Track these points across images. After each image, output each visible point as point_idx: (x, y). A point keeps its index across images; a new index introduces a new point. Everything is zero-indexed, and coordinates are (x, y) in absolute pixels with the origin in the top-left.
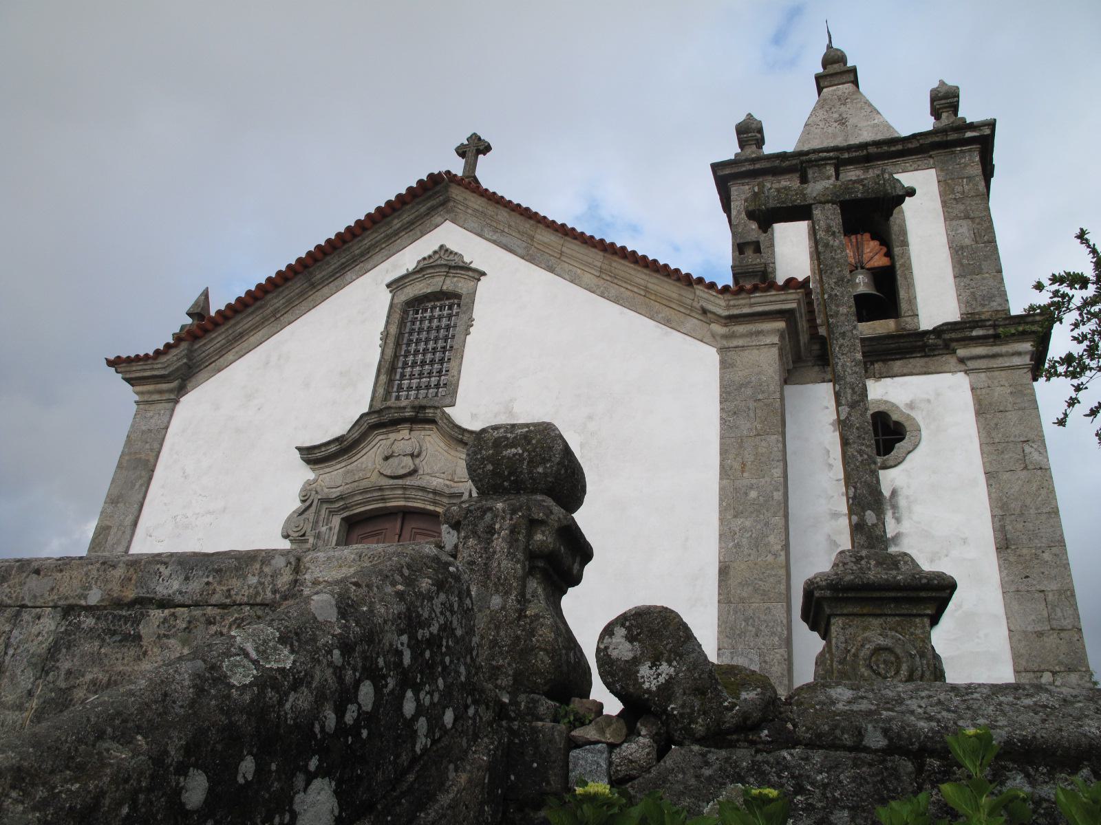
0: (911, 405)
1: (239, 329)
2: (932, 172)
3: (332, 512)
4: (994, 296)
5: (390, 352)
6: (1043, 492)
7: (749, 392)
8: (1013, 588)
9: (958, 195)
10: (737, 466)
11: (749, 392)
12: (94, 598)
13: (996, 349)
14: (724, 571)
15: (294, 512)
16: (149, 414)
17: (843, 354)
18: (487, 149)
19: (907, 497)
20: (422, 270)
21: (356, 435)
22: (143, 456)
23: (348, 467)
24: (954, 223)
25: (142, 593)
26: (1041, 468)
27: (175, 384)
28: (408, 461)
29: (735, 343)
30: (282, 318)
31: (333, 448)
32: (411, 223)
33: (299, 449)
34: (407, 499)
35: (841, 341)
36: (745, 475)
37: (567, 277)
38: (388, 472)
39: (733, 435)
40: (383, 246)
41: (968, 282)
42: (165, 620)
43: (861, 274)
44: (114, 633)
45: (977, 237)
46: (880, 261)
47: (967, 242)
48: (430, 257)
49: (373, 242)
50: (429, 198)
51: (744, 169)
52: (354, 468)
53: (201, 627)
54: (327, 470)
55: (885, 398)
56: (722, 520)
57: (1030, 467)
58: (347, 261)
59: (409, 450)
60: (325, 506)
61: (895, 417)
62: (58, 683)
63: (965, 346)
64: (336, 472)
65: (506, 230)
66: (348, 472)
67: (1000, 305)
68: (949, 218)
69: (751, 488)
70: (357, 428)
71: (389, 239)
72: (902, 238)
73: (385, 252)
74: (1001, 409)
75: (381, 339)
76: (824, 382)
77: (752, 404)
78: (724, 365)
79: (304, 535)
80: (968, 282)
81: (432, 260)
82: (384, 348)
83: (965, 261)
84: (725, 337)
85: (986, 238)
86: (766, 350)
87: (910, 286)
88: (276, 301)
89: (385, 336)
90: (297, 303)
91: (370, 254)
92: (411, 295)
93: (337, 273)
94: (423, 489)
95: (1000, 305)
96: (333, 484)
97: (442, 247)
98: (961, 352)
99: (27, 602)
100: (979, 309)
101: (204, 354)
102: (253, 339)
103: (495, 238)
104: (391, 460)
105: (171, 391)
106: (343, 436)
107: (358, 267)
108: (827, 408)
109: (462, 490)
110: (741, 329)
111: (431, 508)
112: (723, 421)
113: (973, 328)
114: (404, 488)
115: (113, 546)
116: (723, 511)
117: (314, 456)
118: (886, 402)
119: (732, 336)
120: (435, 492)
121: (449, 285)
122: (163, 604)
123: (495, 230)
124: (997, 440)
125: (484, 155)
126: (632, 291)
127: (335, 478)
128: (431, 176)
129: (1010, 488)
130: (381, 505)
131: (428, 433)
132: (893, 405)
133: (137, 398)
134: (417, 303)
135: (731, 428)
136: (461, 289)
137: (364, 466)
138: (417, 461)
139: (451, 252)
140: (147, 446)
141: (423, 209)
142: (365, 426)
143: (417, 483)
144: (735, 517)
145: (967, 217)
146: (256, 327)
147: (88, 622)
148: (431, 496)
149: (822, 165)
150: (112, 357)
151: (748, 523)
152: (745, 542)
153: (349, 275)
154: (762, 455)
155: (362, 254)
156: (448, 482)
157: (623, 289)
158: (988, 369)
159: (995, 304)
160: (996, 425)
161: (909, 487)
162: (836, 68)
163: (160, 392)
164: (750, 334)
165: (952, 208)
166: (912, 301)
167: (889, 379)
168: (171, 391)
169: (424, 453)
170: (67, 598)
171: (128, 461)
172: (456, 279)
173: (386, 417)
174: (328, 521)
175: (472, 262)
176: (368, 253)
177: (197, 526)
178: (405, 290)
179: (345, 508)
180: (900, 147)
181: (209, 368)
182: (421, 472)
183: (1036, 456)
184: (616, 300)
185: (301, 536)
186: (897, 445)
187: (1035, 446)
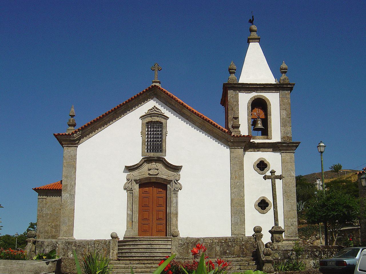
7: (237, 159)
8: (285, 202)
14: (232, 200)
48: (152, 109)
77: (237, 162)
79: (131, 189)
89: (142, 133)
98: (280, 148)
110: (235, 144)
114: (156, 178)
117: (129, 169)
118: (263, 158)
123: (170, 104)
134: (148, 123)
139: (158, 109)
159: (289, 135)
175: (164, 113)
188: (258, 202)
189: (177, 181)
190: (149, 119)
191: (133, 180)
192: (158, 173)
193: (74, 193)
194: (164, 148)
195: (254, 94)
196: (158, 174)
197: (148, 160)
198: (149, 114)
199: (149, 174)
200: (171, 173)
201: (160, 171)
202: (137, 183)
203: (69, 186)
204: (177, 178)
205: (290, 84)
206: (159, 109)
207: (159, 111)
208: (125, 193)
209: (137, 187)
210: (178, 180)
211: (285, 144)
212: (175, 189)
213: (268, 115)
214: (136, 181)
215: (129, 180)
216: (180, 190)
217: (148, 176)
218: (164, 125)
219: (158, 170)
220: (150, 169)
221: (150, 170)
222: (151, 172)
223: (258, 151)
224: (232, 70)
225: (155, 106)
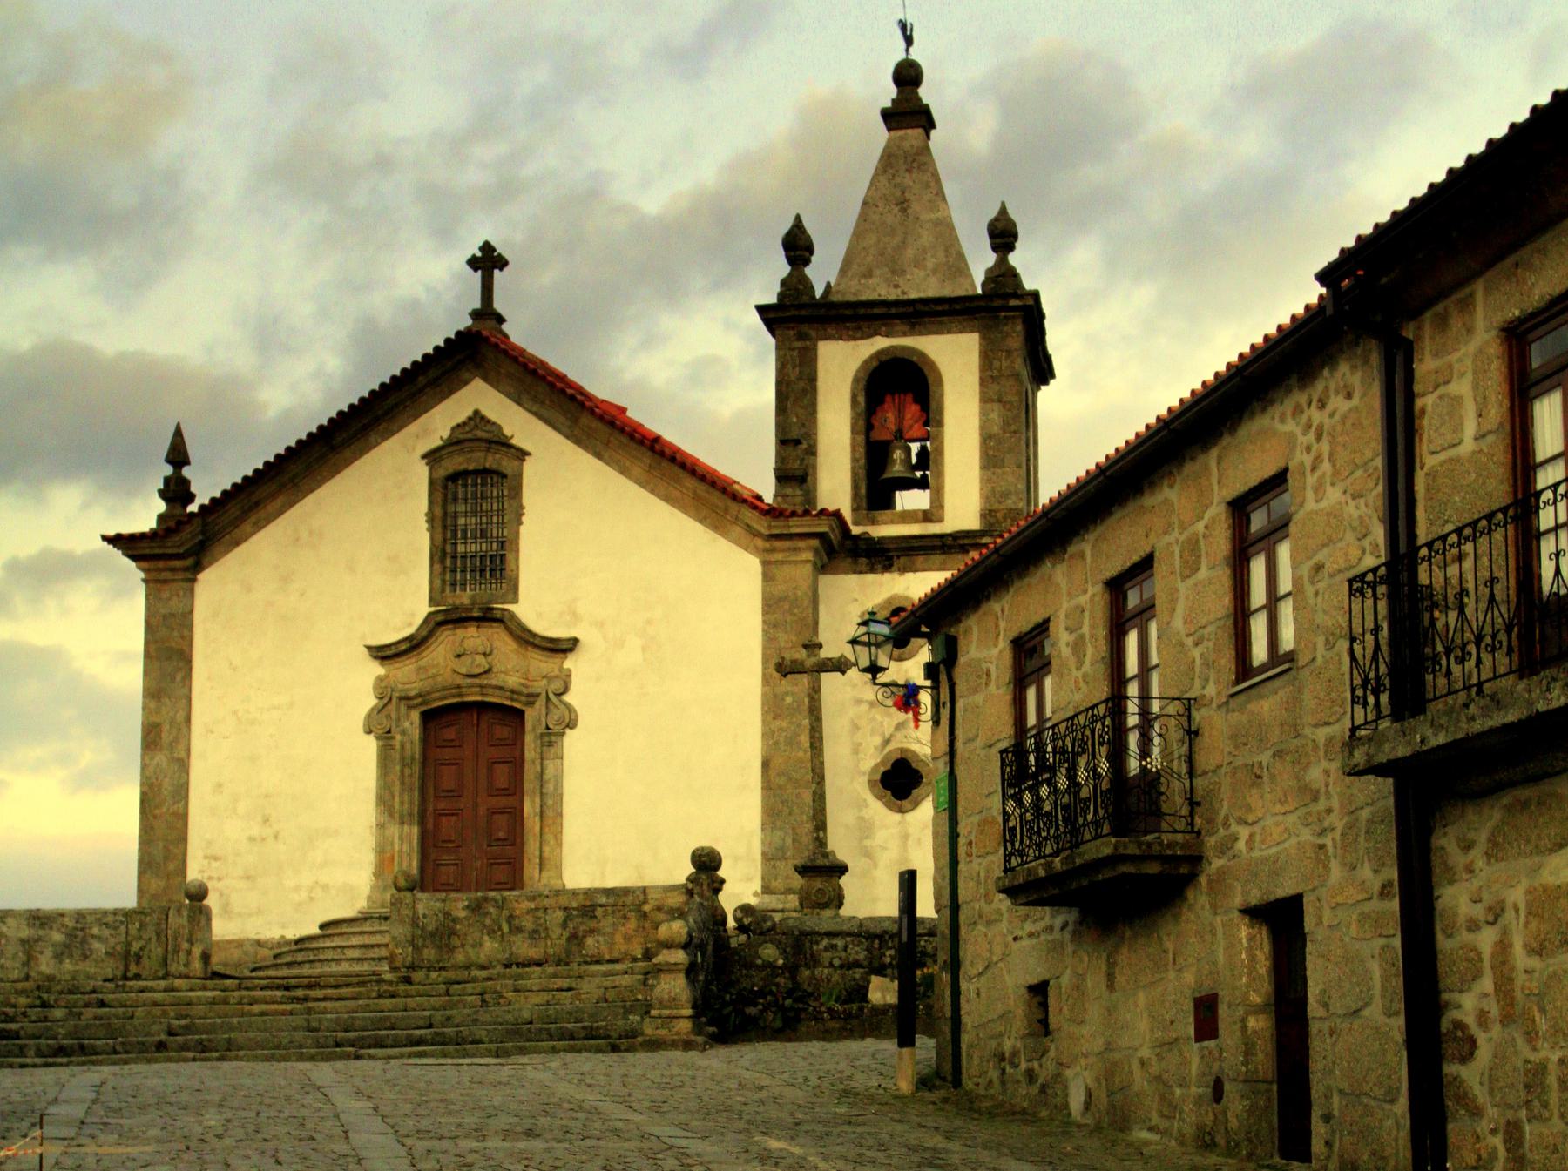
1: (254, 498)
2: (975, 337)
3: (410, 707)
5: (439, 537)
9: (996, 373)
11: (787, 606)
12: (574, 905)
14: (766, 765)
15: (373, 709)
16: (166, 595)
18: (502, 263)
20: (459, 442)
21: (424, 633)
22: (174, 645)
24: (988, 405)
27: (189, 562)
28: (480, 659)
29: (779, 556)
31: (403, 647)
32: (437, 379)
33: (369, 648)
34: (483, 694)
38: (464, 671)
47: (995, 430)
48: (464, 424)
51: (788, 314)
54: (397, 665)
55: (906, 594)
56: (764, 722)
59: (481, 649)
60: (403, 702)
68: (985, 399)
69: (787, 694)
78: (767, 577)
79: (389, 732)
81: (467, 429)
82: (432, 529)
83: (991, 453)
84: (766, 551)
89: (431, 518)
92: (451, 471)
94: (501, 688)
96: (406, 680)
97: (477, 412)
100: (996, 506)
103: (534, 409)
104: (463, 658)
105: (186, 569)
109: (539, 690)
110: (778, 544)
111: (508, 703)
112: (765, 632)
114: (481, 686)
115: (171, 744)
116: (765, 713)
117: (383, 654)
119: (773, 550)
120: (513, 691)
121: (490, 461)
127: (406, 673)
134: (454, 477)
138: (490, 658)
140: (176, 633)
141: (449, 364)
142: (432, 624)
143: (494, 682)
144: (774, 718)
145: (1000, 401)
146: (273, 496)
147: (575, 913)
151: (784, 724)
152: (782, 740)
155: (386, 413)
159: (1010, 502)
163: (173, 570)
164: (789, 549)
168: (186, 569)
169: (495, 652)
173: (453, 616)
174: (408, 716)
180: (946, 307)
182: (495, 670)
184: (667, 499)
188: (882, 769)
189: (559, 695)
191: (394, 700)
193: (183, 754)
195: (880, 343)
196: (485, 672)
197: (445, 619)
198: (458, 441)
200: (541, 664)
203: (166, 727)
207: (494, 428)
208: (370, 747)
209: (412, 723)
216: (571, 728)
225: (477, 412)
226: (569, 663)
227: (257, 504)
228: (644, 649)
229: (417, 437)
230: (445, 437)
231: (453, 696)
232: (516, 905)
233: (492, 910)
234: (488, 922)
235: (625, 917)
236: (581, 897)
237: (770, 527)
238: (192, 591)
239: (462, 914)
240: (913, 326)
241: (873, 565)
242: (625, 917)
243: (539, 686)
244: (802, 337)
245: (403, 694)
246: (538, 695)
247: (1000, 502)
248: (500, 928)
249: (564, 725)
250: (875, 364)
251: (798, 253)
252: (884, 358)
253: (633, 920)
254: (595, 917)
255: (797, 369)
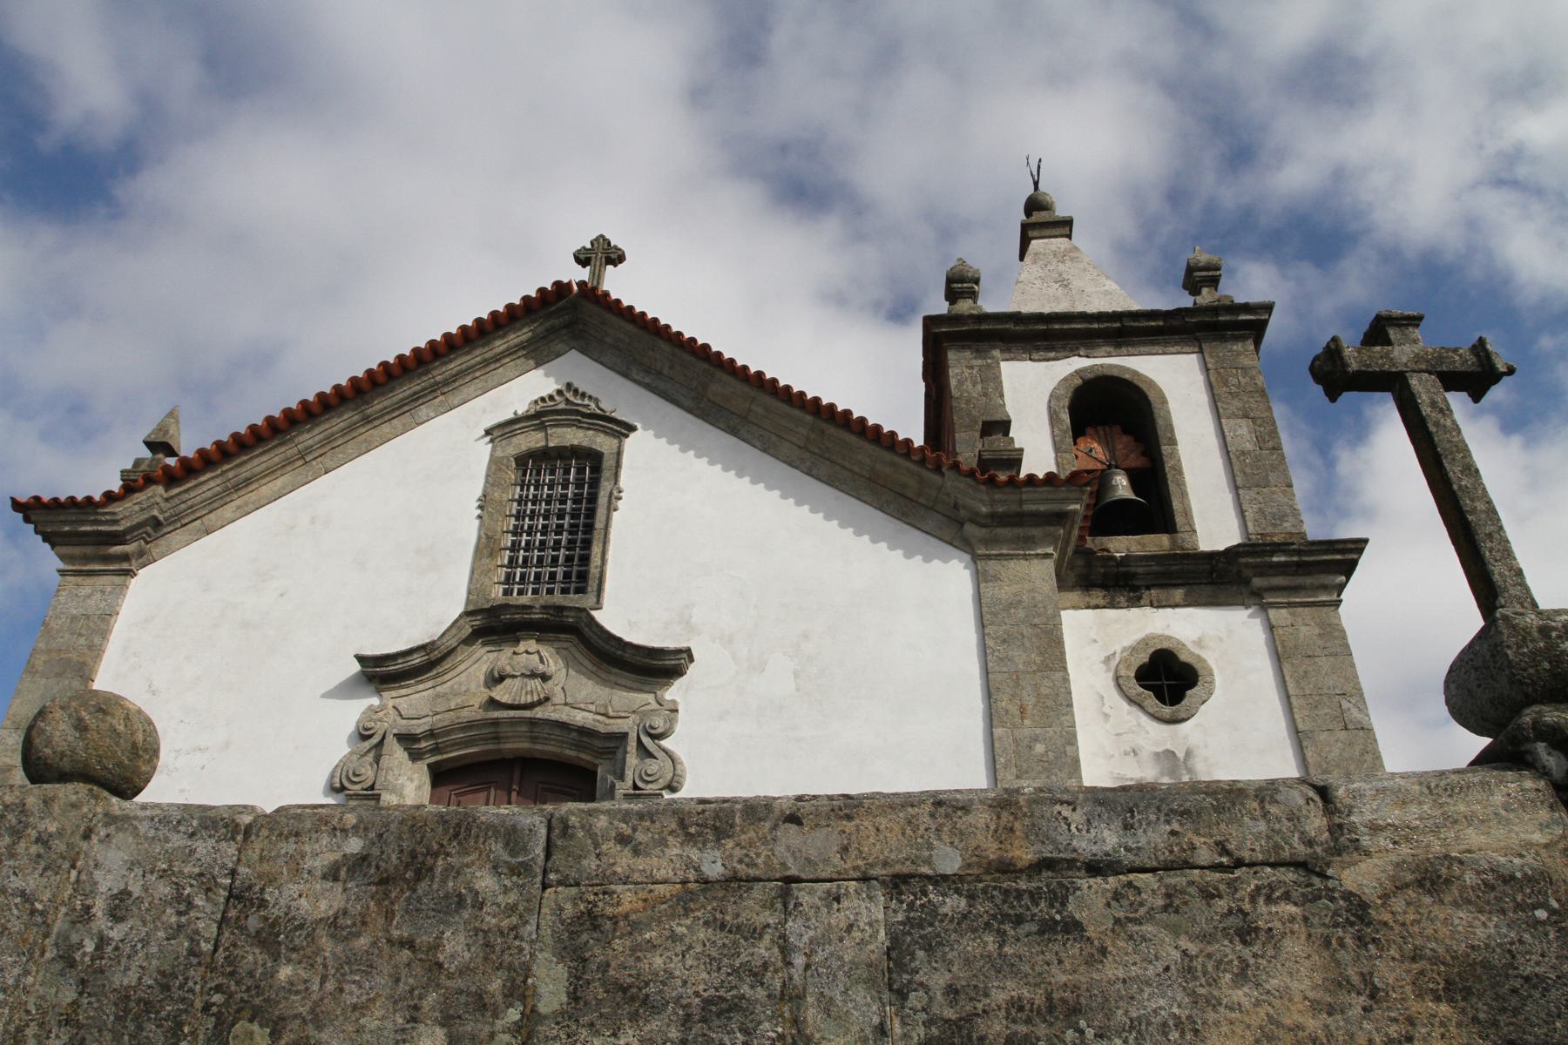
0: (1199, 643)
1: (245, 472)
4: (1286, 515)
6: (1369, 758)
10: (1014, 710)
11: (1021, 614)
13: (1299, 580)
17: (1496, 561)
19: (1206, 760)
22: (74, 656)
23: (438, 689)
25: (1047, 852)
26: (1363, 728)
30: (314, 463)
31: (416, 660)
35: (1489, 544)
36: (1027, 722)
37: (758, 444)
39: (1005, 669)
40: (477, 374)
41: (1254, 496)
42: (1117, 896)
43: (1119, 474)
44: (1019, 921)
45: (1260, 440)
46: (1135, 461)
47: (1249, 446)
48: (551, 397)
49: (464, 366)
50: (550, 315)
52: (448, 690)
53: (1198, 903)
54: (403, 691)
55: (1167, 633)
57: (1350, 726)
58: (423, 390)
61: (1183, 657)
62: (935, 1010)
63: (1261, 575)
64: (417, 695)
65: (666, 371)
66: (438, 696)
67: (1294, 526)
69: (1036, 739)
70: (454, 631)
71: (487, 365)
72: (1169, 435)
73: (479, 384)
74: (1310, 653)
75: (480, 507)
76: (1088, 607)
77: (1027, 631)
79: (372, 787)
80: (1254, 496)
85: (1270, 444)
86: (1036, 561)
87: (1184, 494)
88: (307, 438)
89: (484, 502)
90: (339, 442)
91: (457, 384)
92: (524, 448)
93: (406, 404)
94: (563, 726)
95: (1294, 526)
96: (413, 713)
98: (1257, 582)
99: (793, 871)
100: (1269, 530)
101: (183, 506)
102: (265, 490)
103: (647, 380)
106: (433, 643)
107: (437, 400)
108: (1095, 641)
109: (625, 729)
110: (1003, 532)
113: (1272, 553)
114: (533, 722)
118: (1169, 638)
122: (1095, 868)
123: (648, 371)
124: (1308, 692)
125: (615, 266)
126: (850, 471)
128: (558, 284)
129: (1329, 752)
130: (490, 747)
131: (565, 645)
132: (1179, 642)
133: (61, 566)
135: (1002, 659)
136: (601, 447)
137: (463, 689)
139: (583, 395)
140: (82, 641)
145: (1246, 416)
146: (270, 473)
147: (953, 904)
148: (574, 735)
149: (1404, 325)
150: (23, 498)
153: (423, 411)
154: (1047, 696)
155: (446, 383)
156: (599, 717)
157: (838, 468)
158: (1290, 605)
160: (1306, 672)
161: (1206, 746)
162: (1038, 217)
165: (1227, 403)
166: (1187, 513)
167: (1169, 610)
170: (885, 864)
171: (45, 662)
172: (591, 432)
176: (454, 381)
177: (177, 770)
178: (514, 439)
179: (436, 750)
181: (188, 527)
183: (1355, 713)
185: (366, 790)
186: (1189, 693)
187: (1354, 701)
190: (532, 440)
191: (390, 739)
192: (547, 699)
194: (594, 571)
196: (540, 703)
198: (539, 416)
199: (493, 704)
201: (559, 688)
202: (415, 756)
204: (659, 723)
205: (1246, 308)
206: (589, 392)
207: (586, 402)
210: (660, 731)
211: (1285, 552)
212: (640, 784)
213: (1163, 440)
214: (406, 739)
215: (370, 736)
217: (480, 715)
218: (608, 463)
219: (545, 678)
220: (501, 679)
221: (496, 679)
222: (502, 693)
223: (1135, 602)
224: (962, 281)
226: (674, 692)
227: (248, 482)
228: (796, 675)
229: (484, 411)
230: (520, 412)
231: (486, 740)
232: (623, 861)
233: (485, 882)
234: (456, 946)
235: (1246, 933)
236: (981, 817)
237: (993, 502)
238: (125, 586)
239: (317, 900)
240: (1118, 346)
241: (1113, 599)
242: (1246, 933)
243: (627, 725)
244: (980, 353)
245: (404, 731)
246: (624, 736)
247: (1275, 525)
248: (519, 990)
249: (662, 783)
250: (1079, 382)
251: (965, 285)
252: (1089, 376)
253: (1294, 947)
254: (1073, 927)
255: (979, 387)
